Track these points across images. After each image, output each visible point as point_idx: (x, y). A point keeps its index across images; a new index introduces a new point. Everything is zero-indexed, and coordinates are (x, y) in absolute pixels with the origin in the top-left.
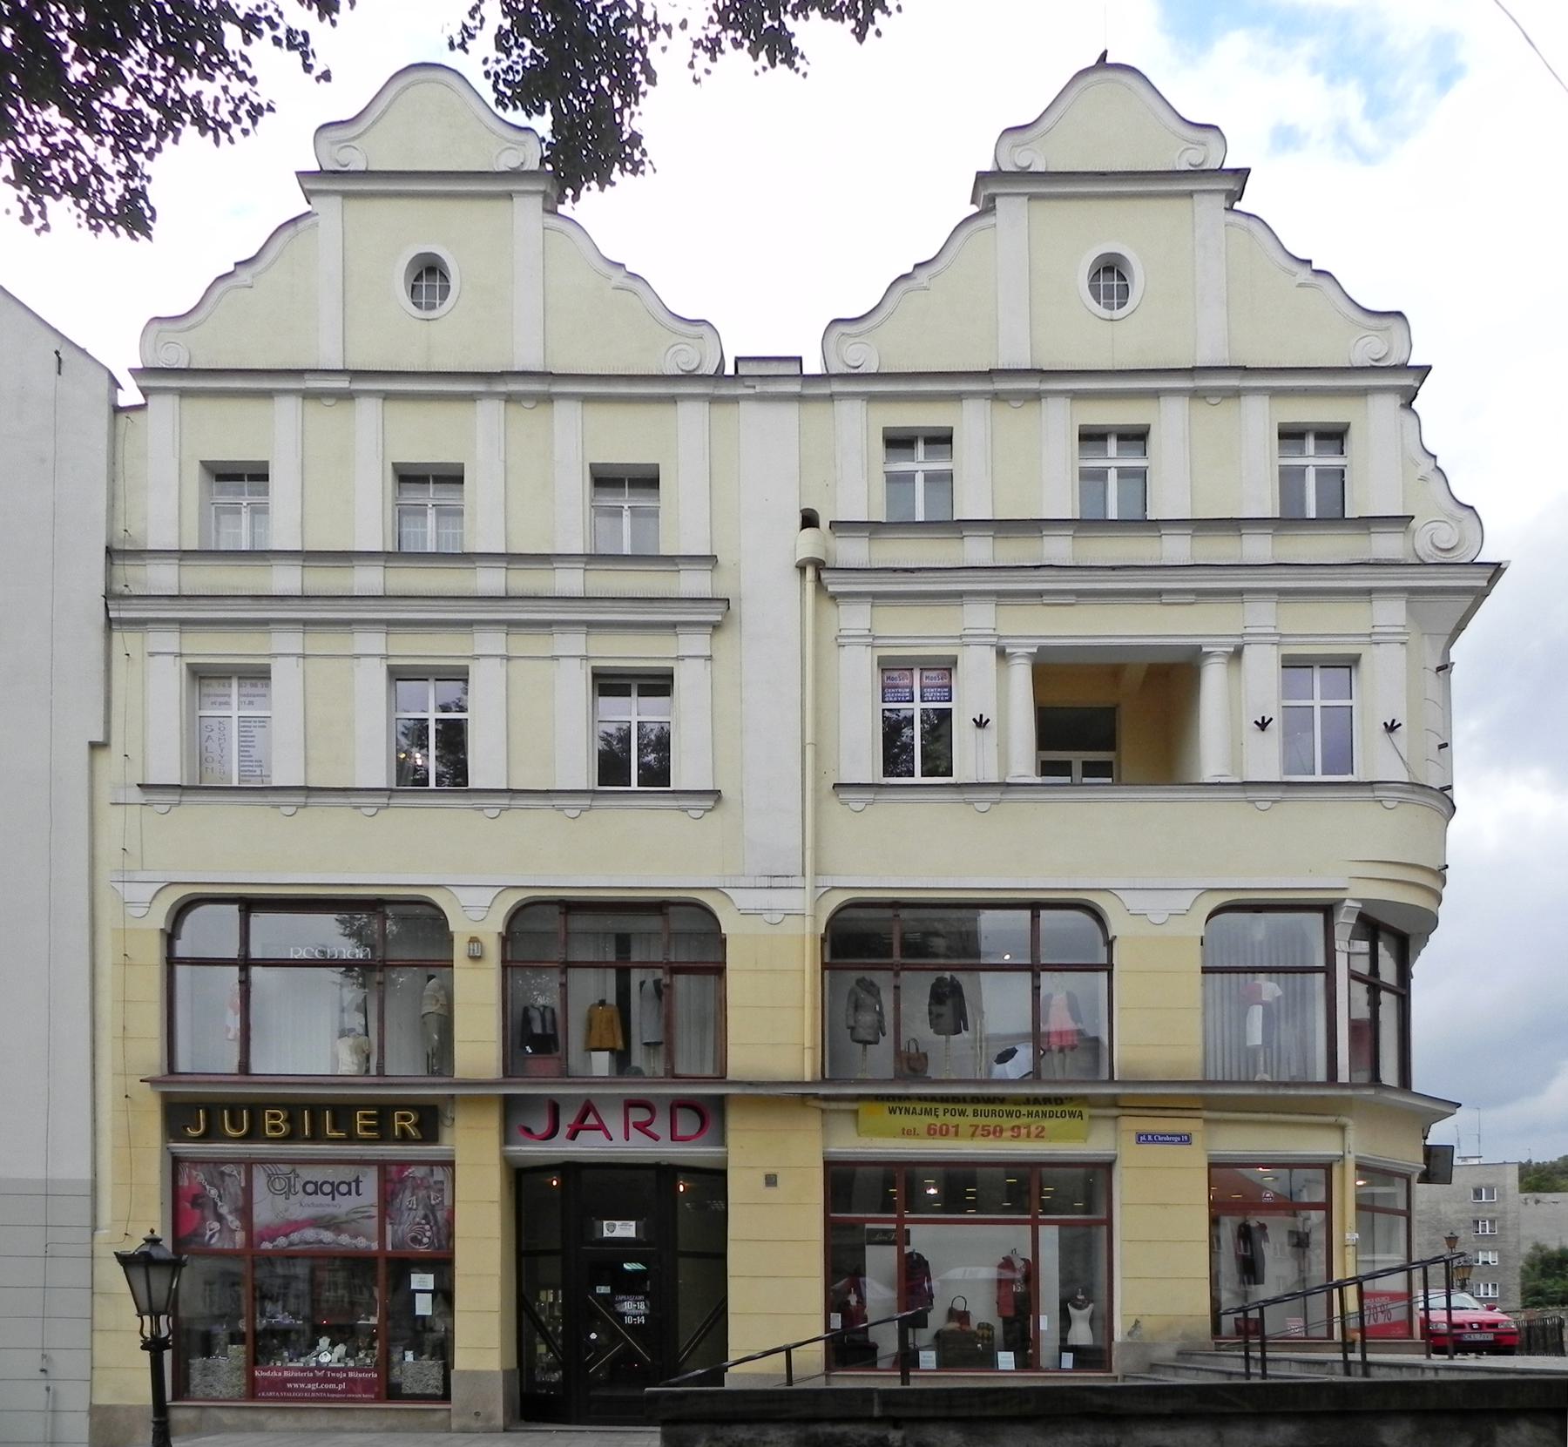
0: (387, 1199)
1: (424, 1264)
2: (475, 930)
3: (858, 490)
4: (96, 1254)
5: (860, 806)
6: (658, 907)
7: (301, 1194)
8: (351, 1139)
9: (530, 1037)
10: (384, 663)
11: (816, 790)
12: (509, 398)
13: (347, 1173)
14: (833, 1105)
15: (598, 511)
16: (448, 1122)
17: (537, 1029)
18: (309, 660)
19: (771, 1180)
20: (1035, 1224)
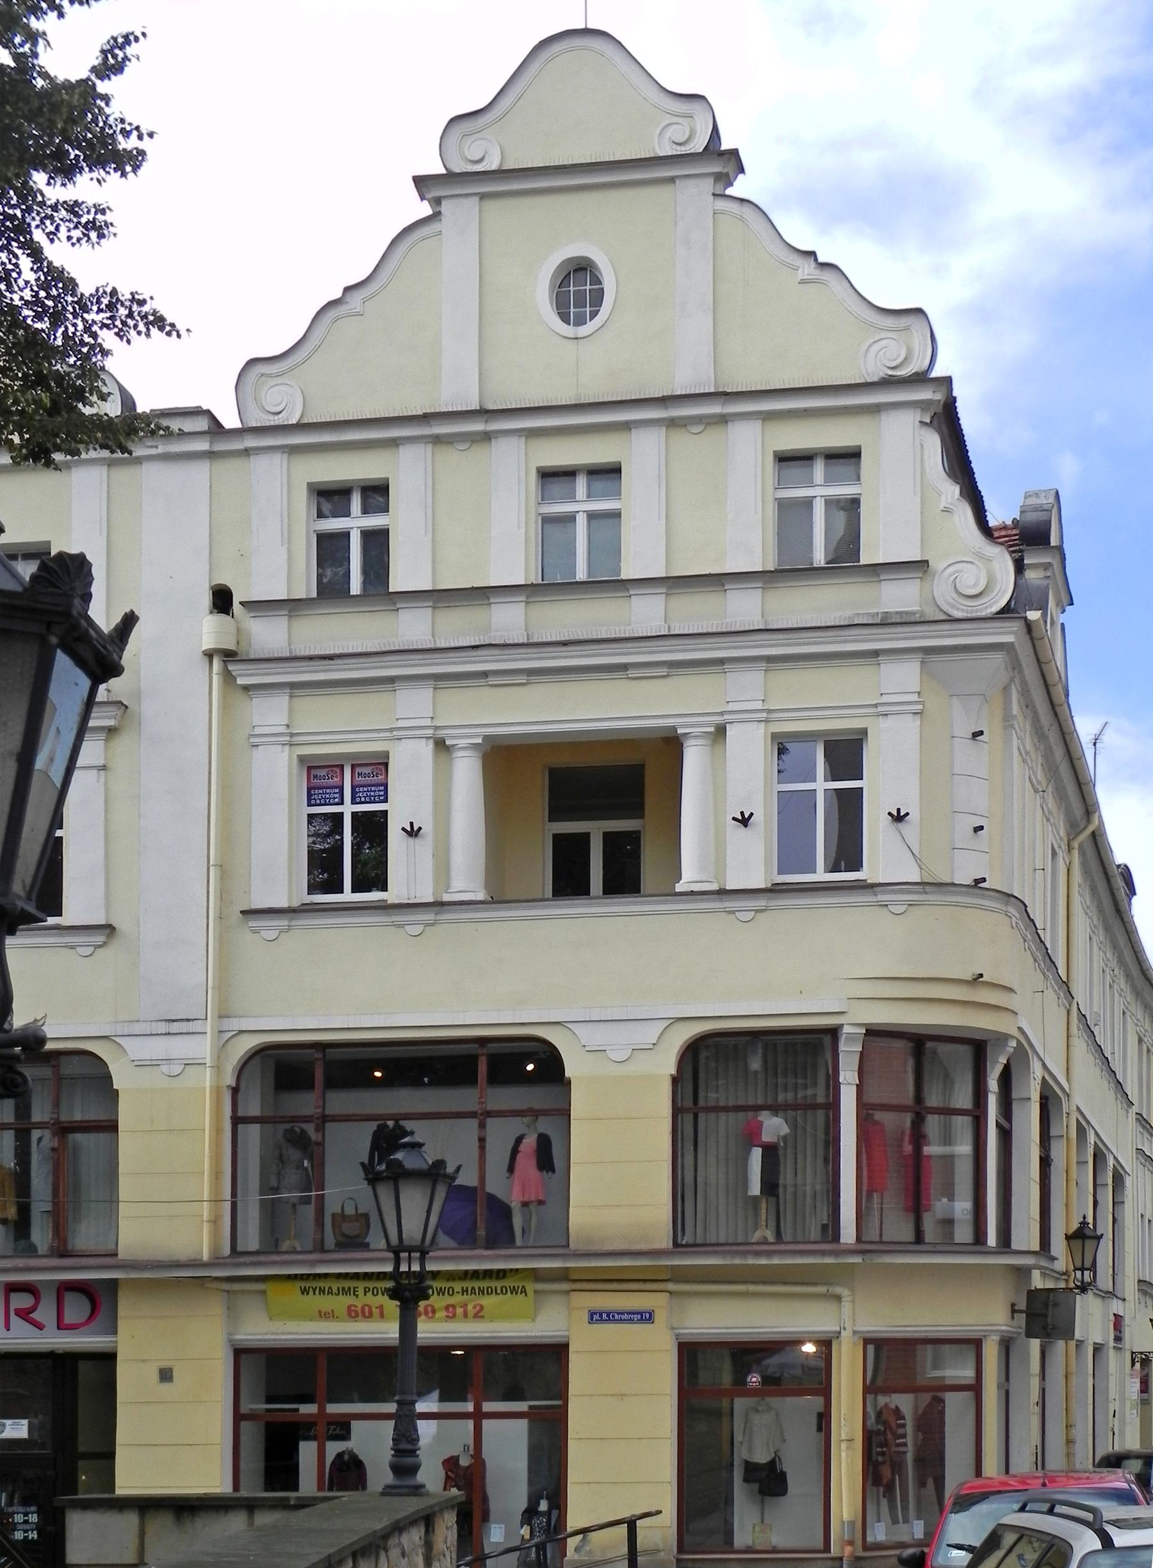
3: (277, 563)
5: (273, 935)
19: (166, 1375)
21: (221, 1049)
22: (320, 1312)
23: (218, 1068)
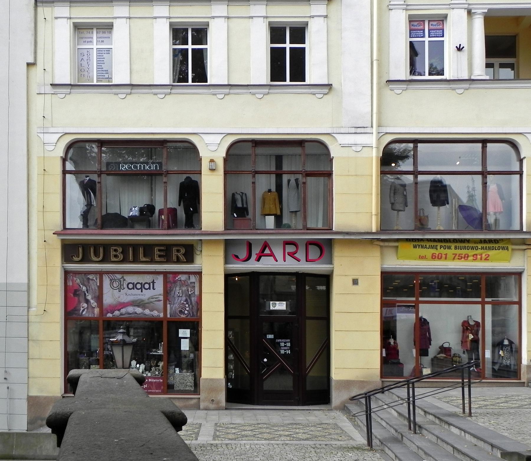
0: (167, 293)
1: (184, 325)
2: (212, 156)
4: (30, 321)
5: (399, 91)
6: (300, 143)
7: (126, 288)
8: (152, 262)
9: (236, 210)
11: (379, 83)
13: (148, 278)
14: (386, 244)
16: (198, 253)
17: (239, 205)
18: (132, 20)
19: (355, 282)
20: (483, 303)
21: (379, 139)
22: (420, 256)
23: (377, 148)
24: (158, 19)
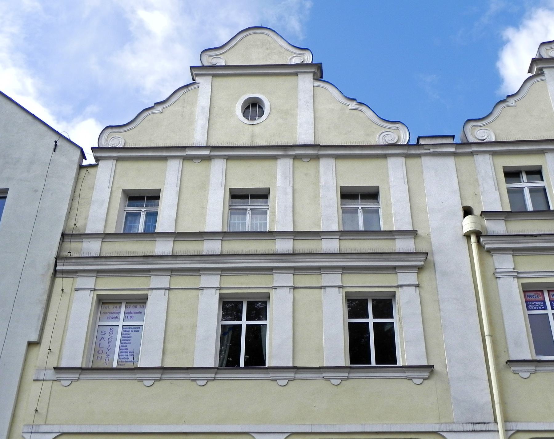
5: (526, 375)
10: (218, 292)
11: (496, 365)
12: (295, 158)
15: (345, 211)
18: (171, 292)
24: (205, 291)
